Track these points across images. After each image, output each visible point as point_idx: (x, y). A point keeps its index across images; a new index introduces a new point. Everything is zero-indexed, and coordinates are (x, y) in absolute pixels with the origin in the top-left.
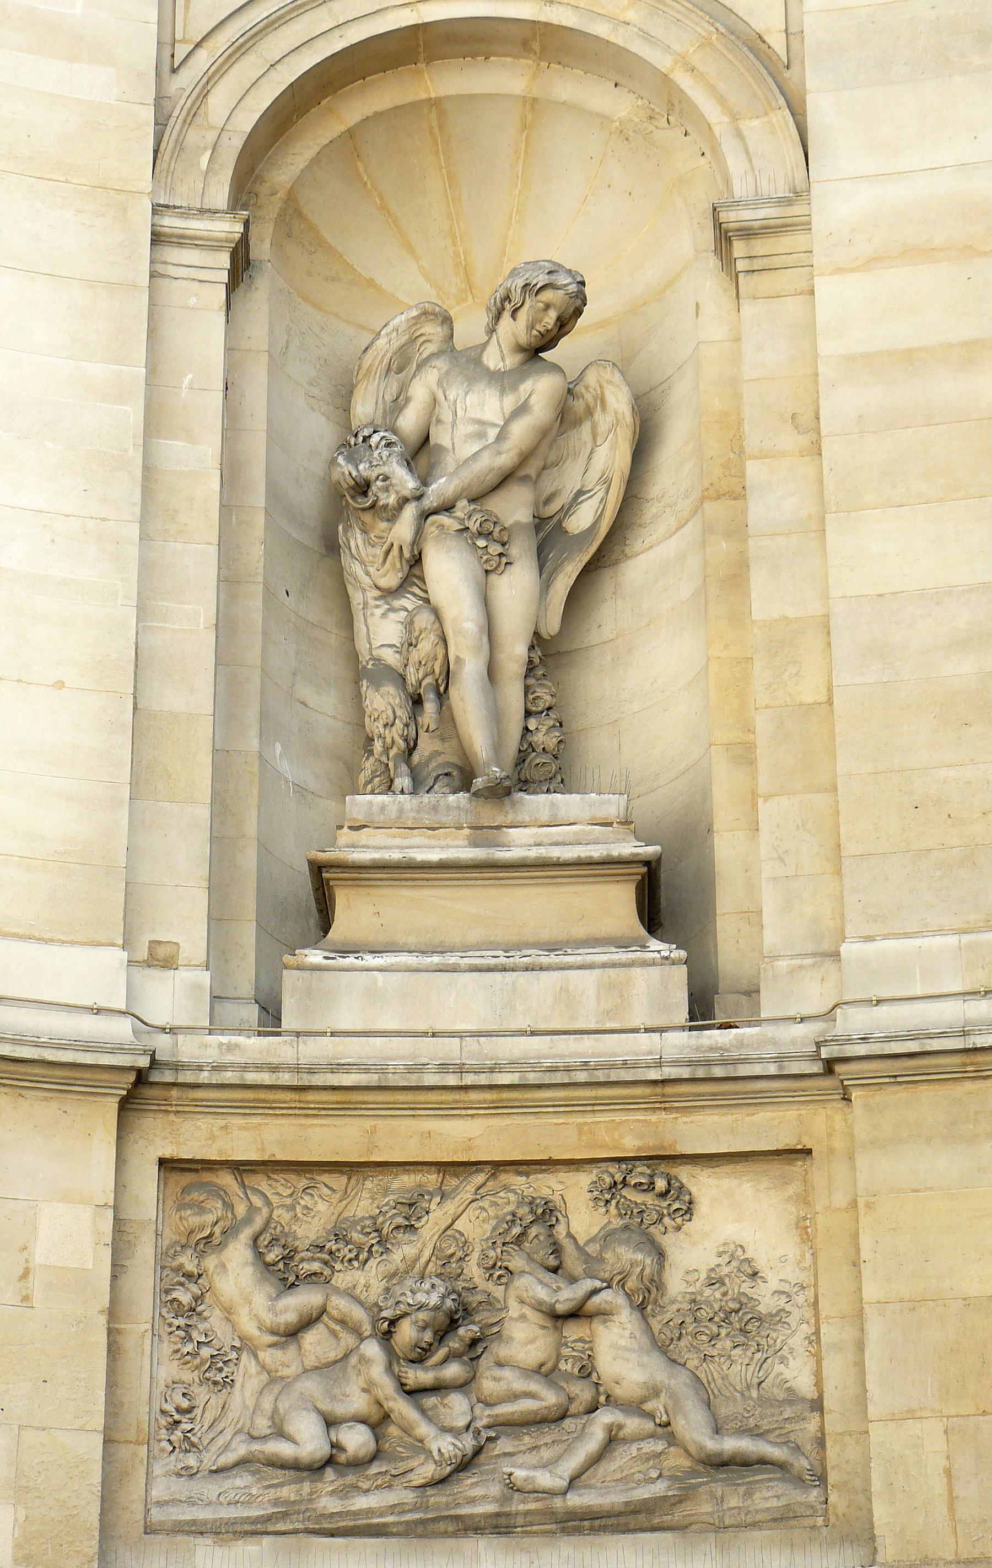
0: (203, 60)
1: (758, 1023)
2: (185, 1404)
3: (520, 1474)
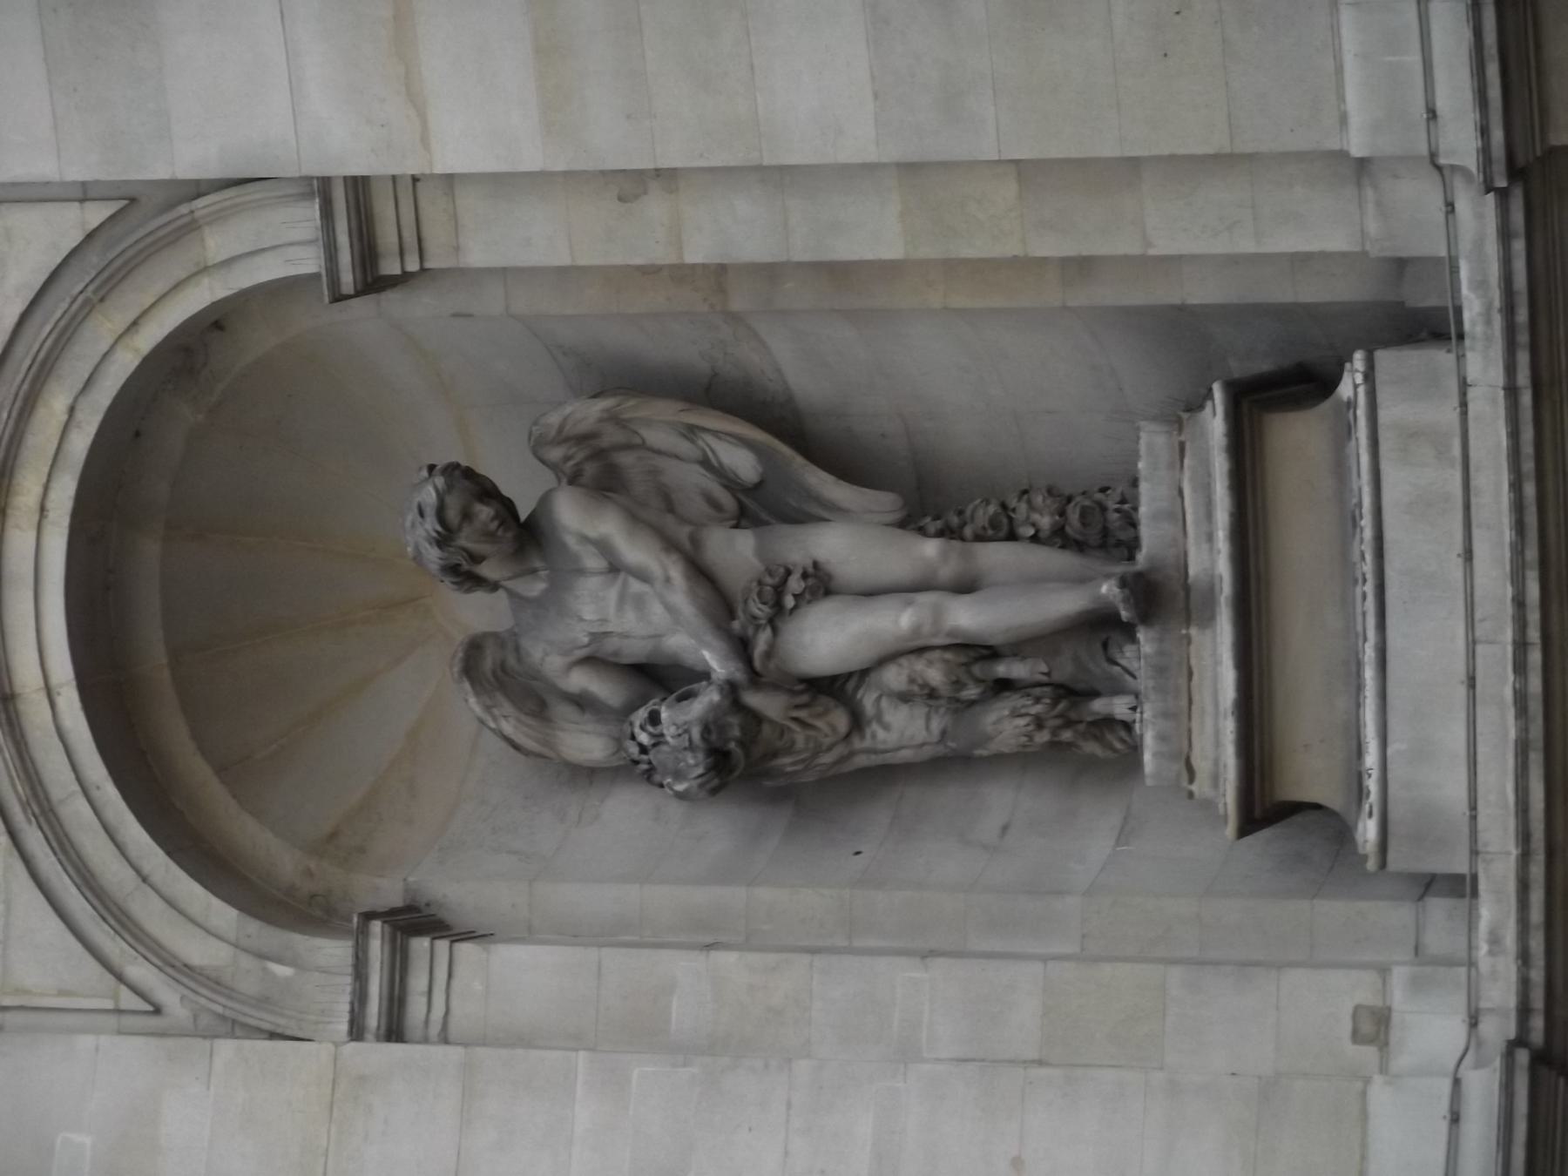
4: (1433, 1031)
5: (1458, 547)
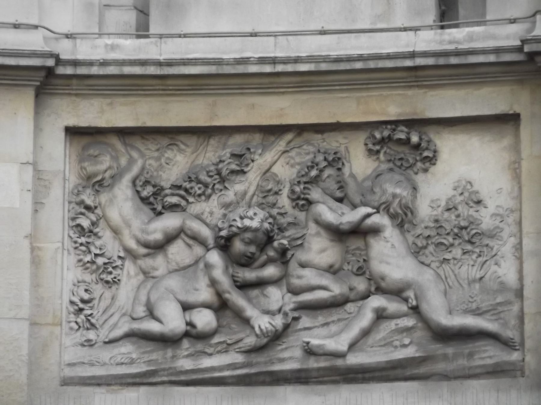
2: (86, 296)
3: (315, 342)
5: (327, 28)
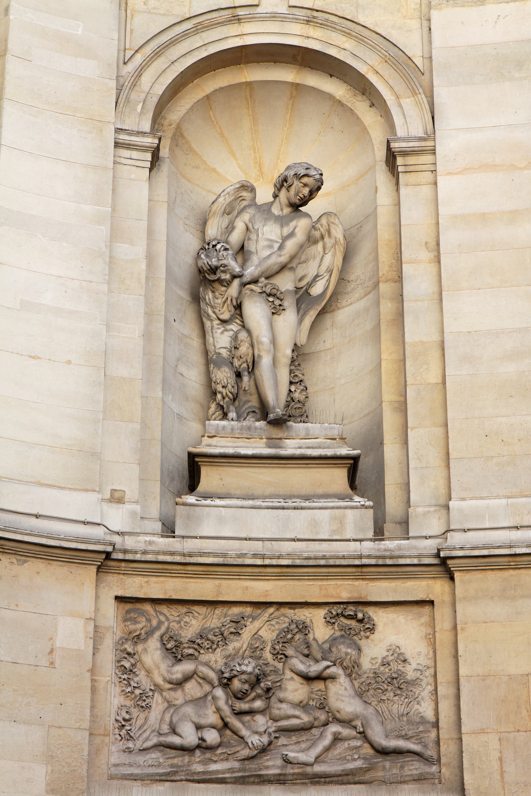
0: (139, 59)
1: (408, 539)
2: (127, 717)
3: (291, 755)
4: (117, 518)
5: (299, 537)
